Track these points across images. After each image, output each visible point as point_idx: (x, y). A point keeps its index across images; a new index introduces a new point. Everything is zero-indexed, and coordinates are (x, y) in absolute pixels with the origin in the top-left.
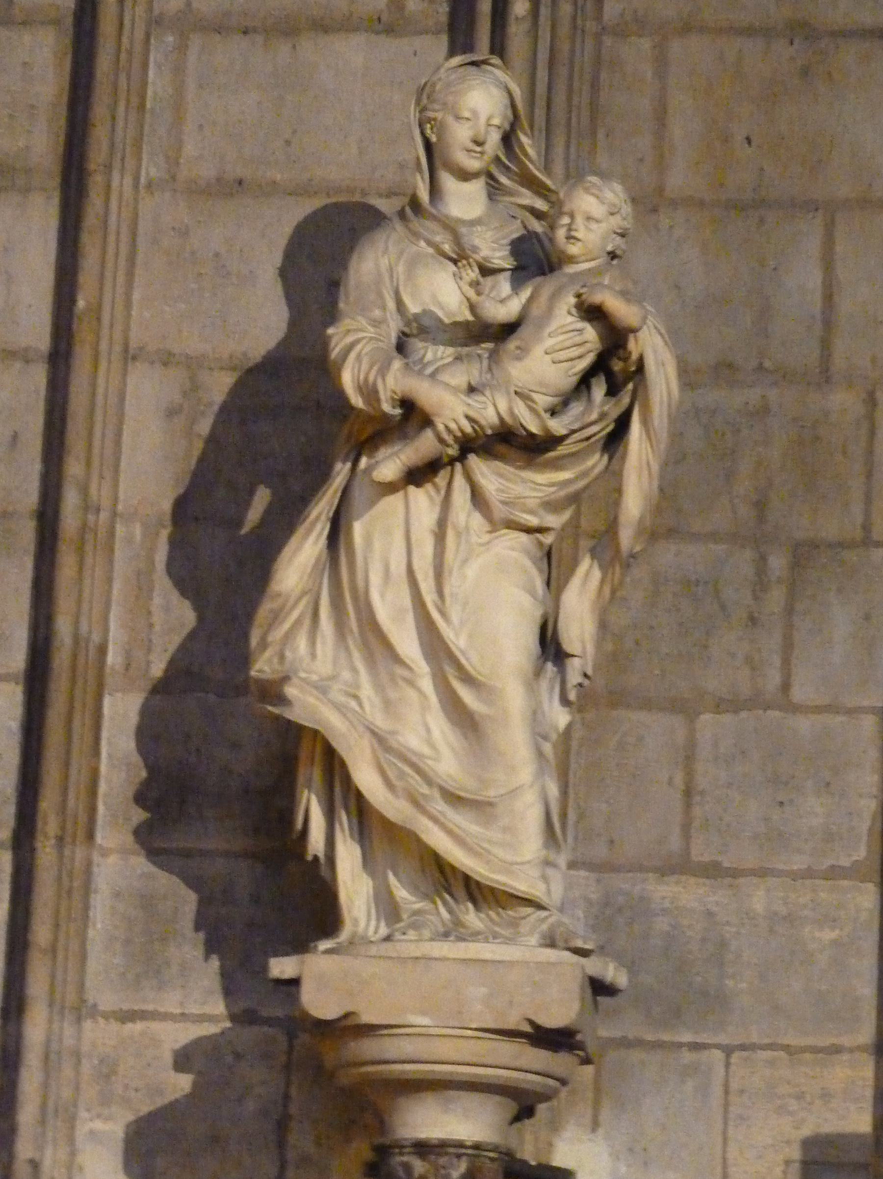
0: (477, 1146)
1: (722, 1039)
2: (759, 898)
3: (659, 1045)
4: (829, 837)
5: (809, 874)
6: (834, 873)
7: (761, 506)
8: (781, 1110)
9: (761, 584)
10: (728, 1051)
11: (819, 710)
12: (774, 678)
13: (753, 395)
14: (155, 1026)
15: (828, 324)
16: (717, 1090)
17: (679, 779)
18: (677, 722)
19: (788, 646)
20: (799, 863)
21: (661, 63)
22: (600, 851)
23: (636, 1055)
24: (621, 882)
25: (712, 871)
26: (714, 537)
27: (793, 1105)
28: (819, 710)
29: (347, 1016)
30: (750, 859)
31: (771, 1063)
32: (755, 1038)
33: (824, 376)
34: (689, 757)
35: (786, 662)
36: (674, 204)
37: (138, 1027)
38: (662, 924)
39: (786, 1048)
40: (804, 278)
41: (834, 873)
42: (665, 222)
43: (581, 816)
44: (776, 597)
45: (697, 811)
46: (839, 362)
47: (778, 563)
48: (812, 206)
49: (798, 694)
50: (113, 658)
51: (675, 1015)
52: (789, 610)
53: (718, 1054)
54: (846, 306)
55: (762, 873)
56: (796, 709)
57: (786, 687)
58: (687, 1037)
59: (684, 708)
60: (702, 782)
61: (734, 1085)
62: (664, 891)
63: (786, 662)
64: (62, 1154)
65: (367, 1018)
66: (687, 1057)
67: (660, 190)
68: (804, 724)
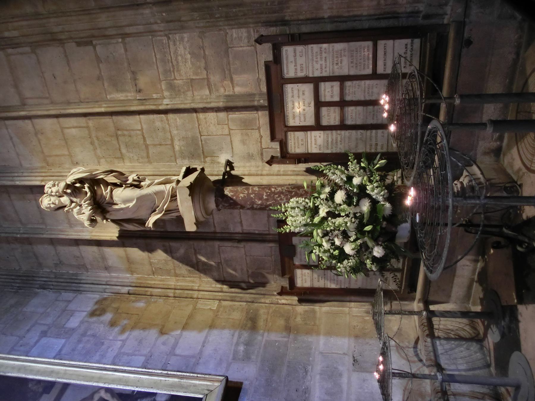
0: (215, 197)
1: (199, 137)
2: (175, 132)
3: (202, 147)
4: (162, 121)
5: (168, 124)
6: (167, 120)
7: (112, 136)
8: (209, 126)
9: (124, 135)
10: (201, 136)
11: (141, 124)
12: (138, 132)
13: (95, 139)
14: (215, 222)
15: (80, 127)
16: (209, 137)
17: (159, 146)
18: (150, 148)
19: (133, 130)
20: (167, 126)
21: (50, 156)
22: (173, 158)
23: (205, 151)
24: (177, 155)
25: (172, 140)
26: (118, 143)
27: (208, 124)
28: (141, 124)
29: (195, 224)
30: (168, 135)
31: (202, 128)
32: (198, 131)
33: (88, 127)
34: (155, 145)
35: (135, 130)
36: (70, 153)
37: (216, 225)
38: (183, 148)
39: (199, 125)
40: (74, 131)
41: (167, 120)
42: (73, 154)
43: (168, 162)
44: (126, 133)
45: (163, 143)
46: (85, 125)
47: (119, 133)
48: (62, 132)
49: (140, 128)
50: (162, 230)
51: (197, 144)
52: (127, 130)
53: (202, 137)
54: (75, 125)
55: (170, 132)
56: (142, 129)
57: (139, 130)
58: (200, 142)
59: (147, 146)
60: (158, 143)
61: (206, 134)
62: (177, 148)
63: (135, 130)
64: (237, 235)
65: (194, 221)
66: (203, 142)
67: (68, 155)
68: (145, 127)
